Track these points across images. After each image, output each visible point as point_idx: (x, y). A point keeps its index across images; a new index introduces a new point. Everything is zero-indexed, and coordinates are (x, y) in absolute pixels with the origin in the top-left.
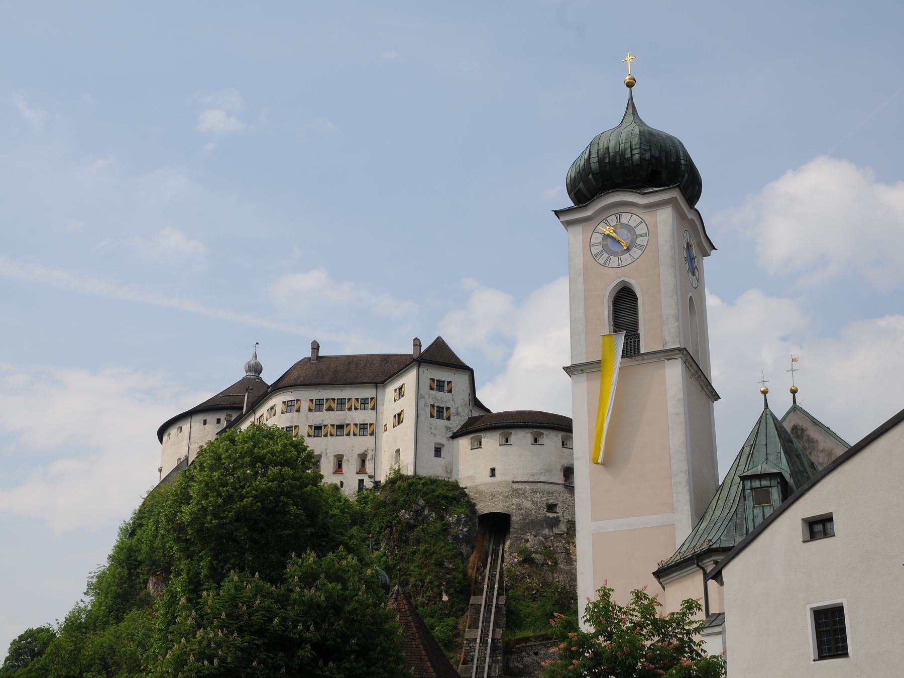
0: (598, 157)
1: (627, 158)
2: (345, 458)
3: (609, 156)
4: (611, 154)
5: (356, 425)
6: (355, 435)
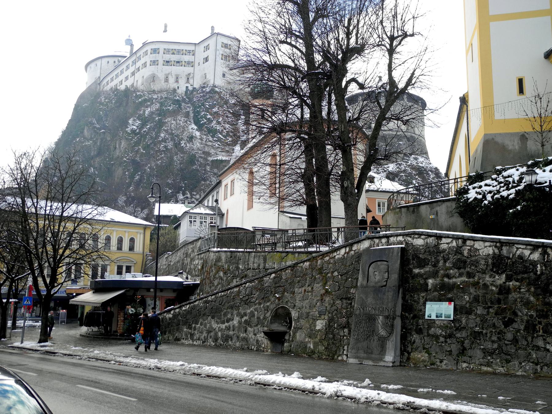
2: (180, 76)
5: (185, 62)
6: (185, 66)
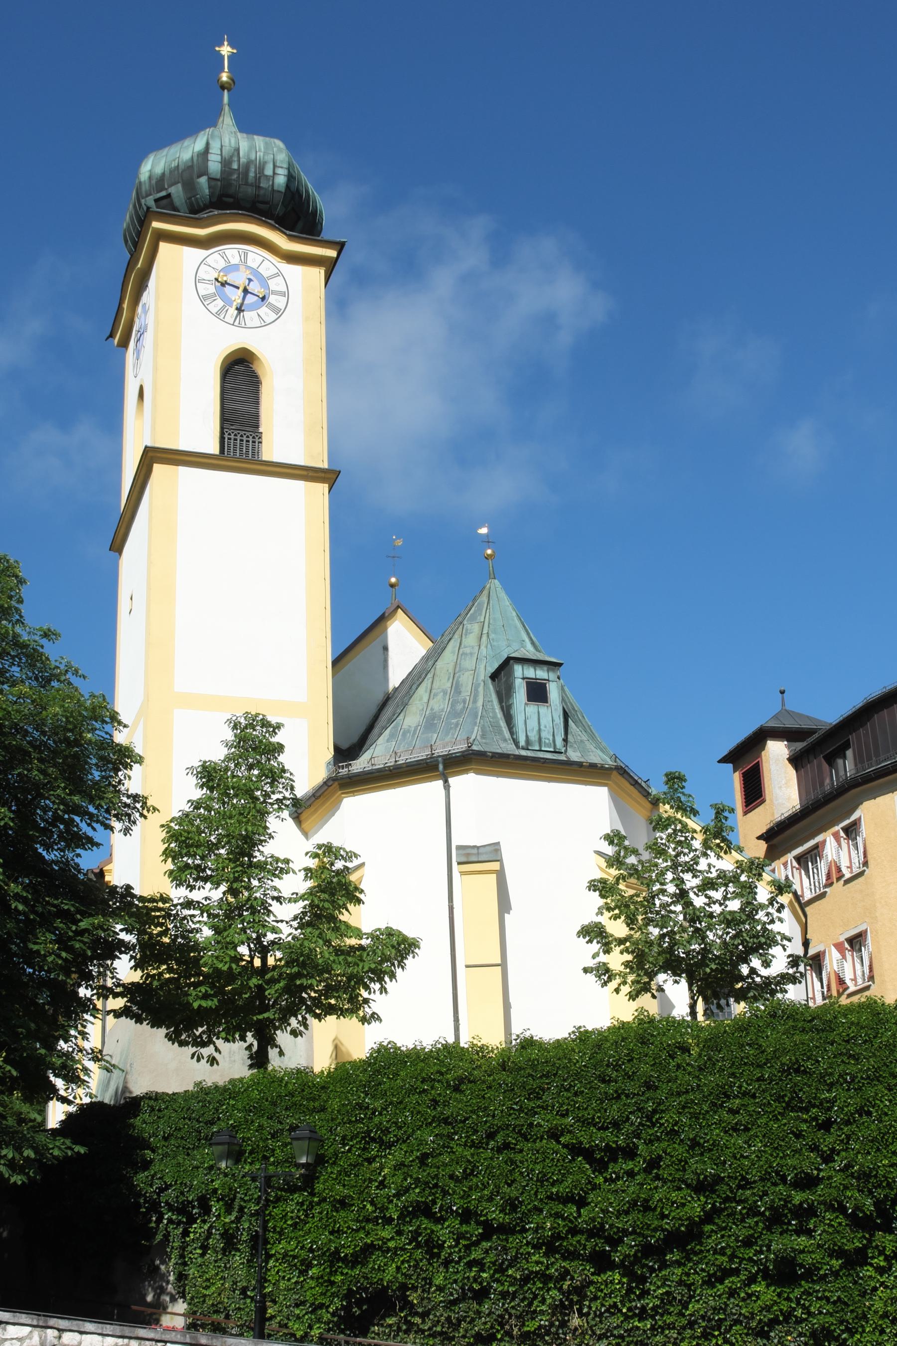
0: (221, 155)
1: (267, 176)
3: (239, 161)
4: (243, 160)
